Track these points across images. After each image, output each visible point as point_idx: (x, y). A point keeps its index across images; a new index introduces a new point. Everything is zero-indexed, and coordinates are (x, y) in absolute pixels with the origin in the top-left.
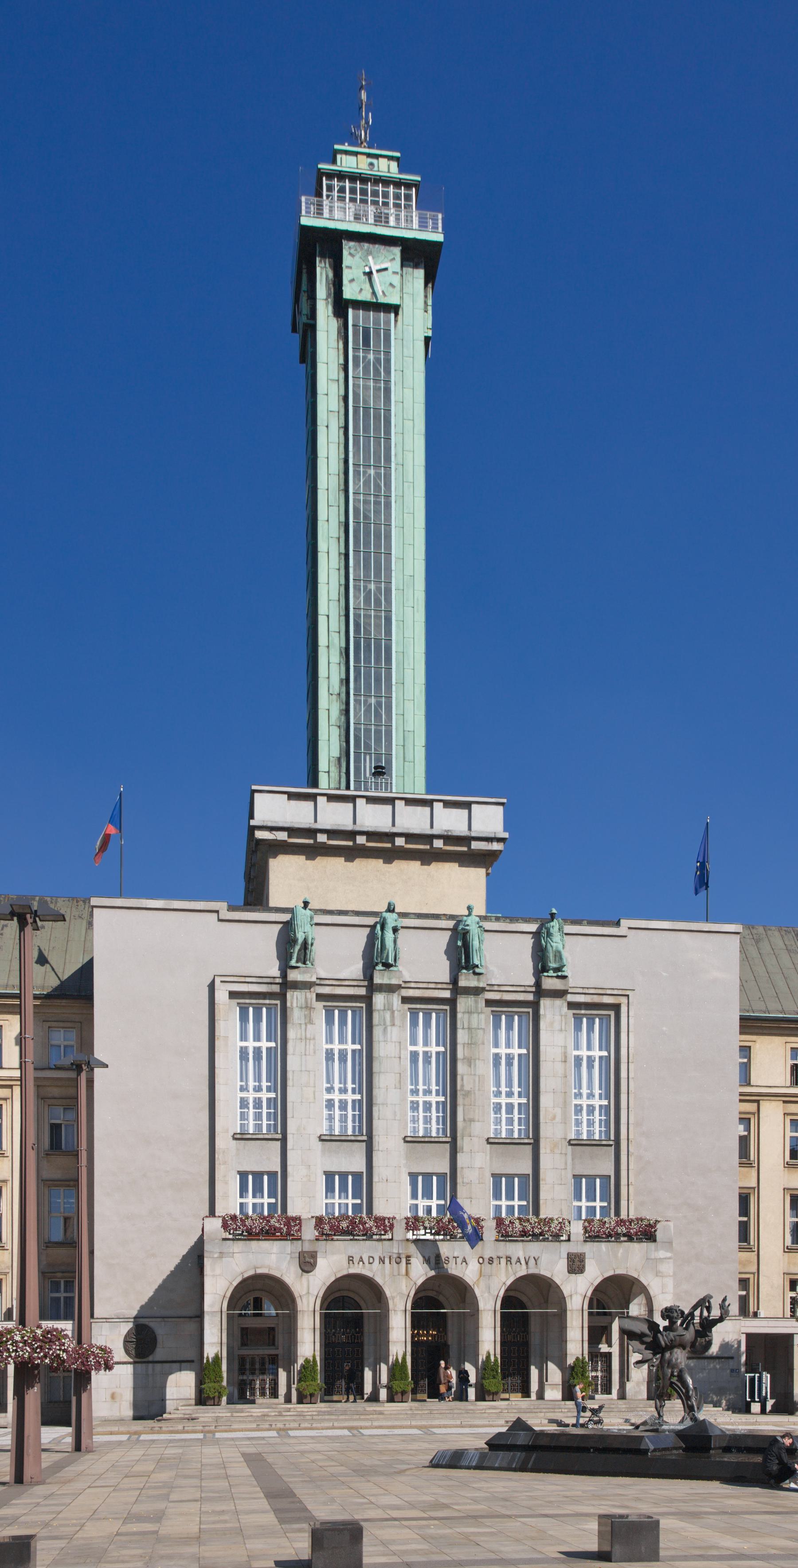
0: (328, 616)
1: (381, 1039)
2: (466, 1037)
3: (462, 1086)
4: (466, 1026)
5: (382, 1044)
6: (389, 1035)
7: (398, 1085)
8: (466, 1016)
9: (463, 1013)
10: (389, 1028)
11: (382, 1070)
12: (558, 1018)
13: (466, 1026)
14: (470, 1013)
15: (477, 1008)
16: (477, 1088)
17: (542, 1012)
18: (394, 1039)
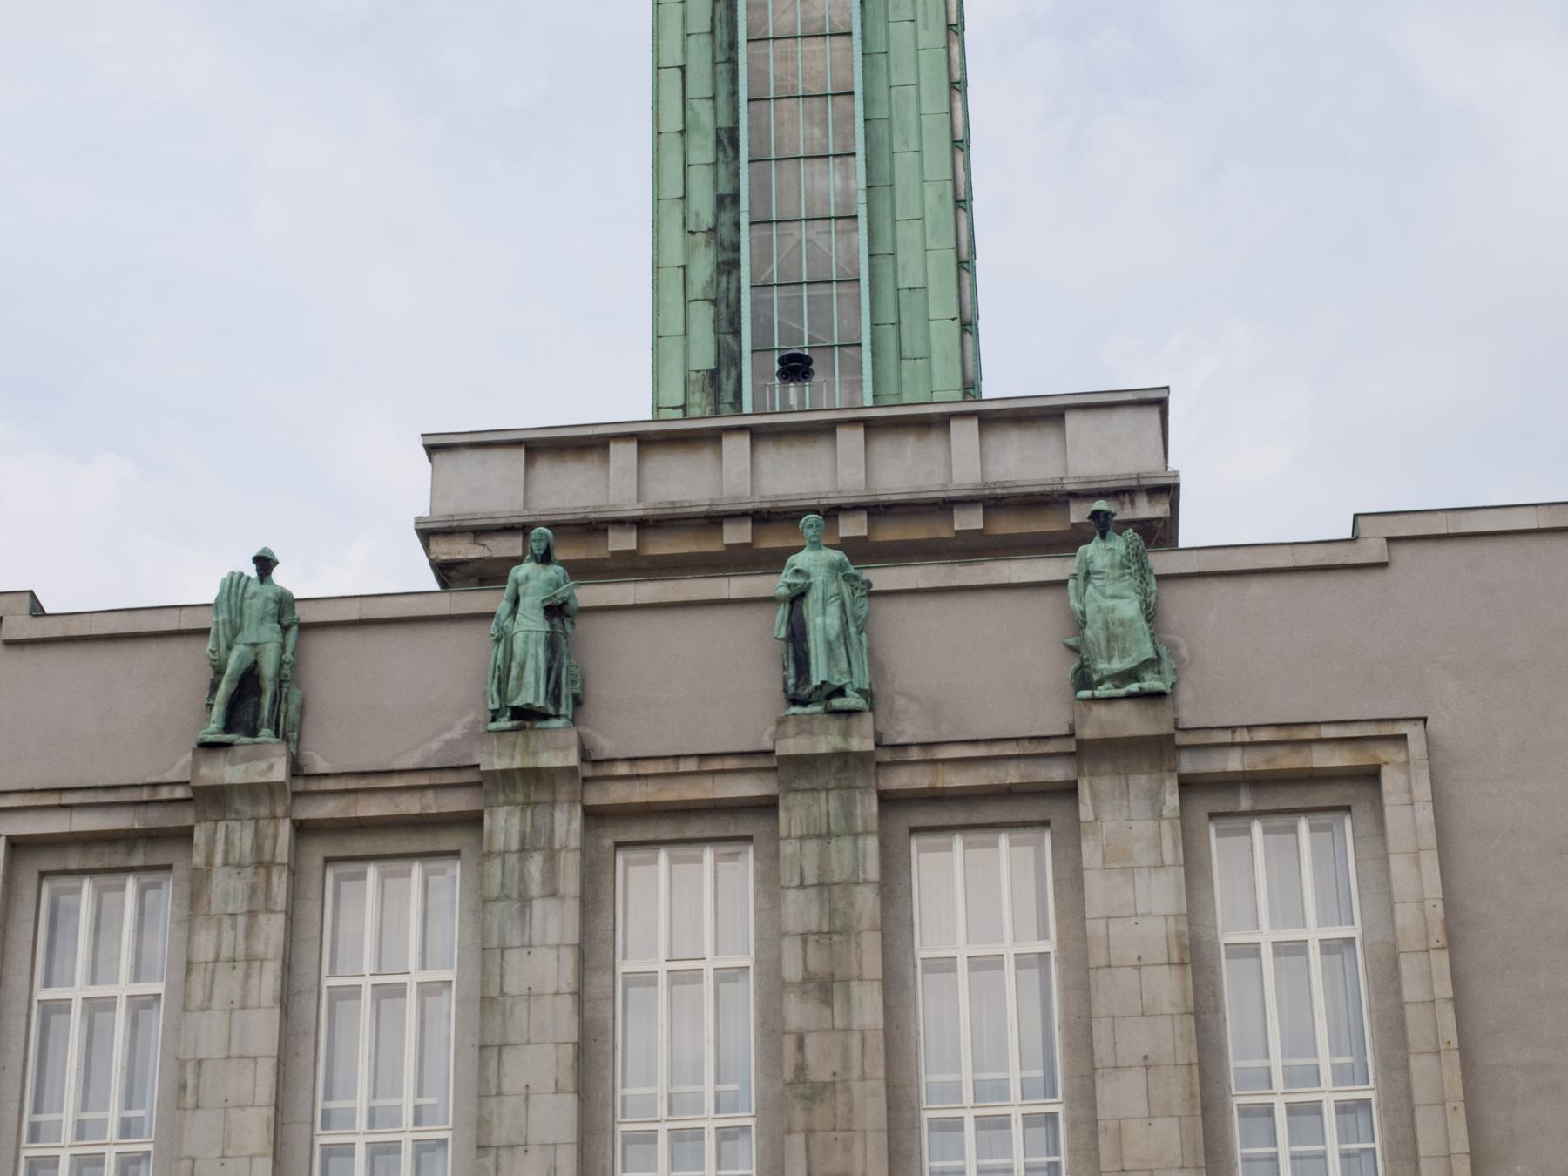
0: (683, 69)
1: (514, 938)
2: (814, 911)
3: (801, 1068)
4: (811, 878)
5: (513, 957)
6: (536, 923)
7: (568, 1082)
8: (812, 846)
9: (802, 838)
10: (538, 905)
11: (513, 1039)
12: (1143, 827)
13: (811, 878)
14: (825, 836)
15: (849, 815)
16: (856, 1072)
17: (1086, 812)
18: (553, 938)
